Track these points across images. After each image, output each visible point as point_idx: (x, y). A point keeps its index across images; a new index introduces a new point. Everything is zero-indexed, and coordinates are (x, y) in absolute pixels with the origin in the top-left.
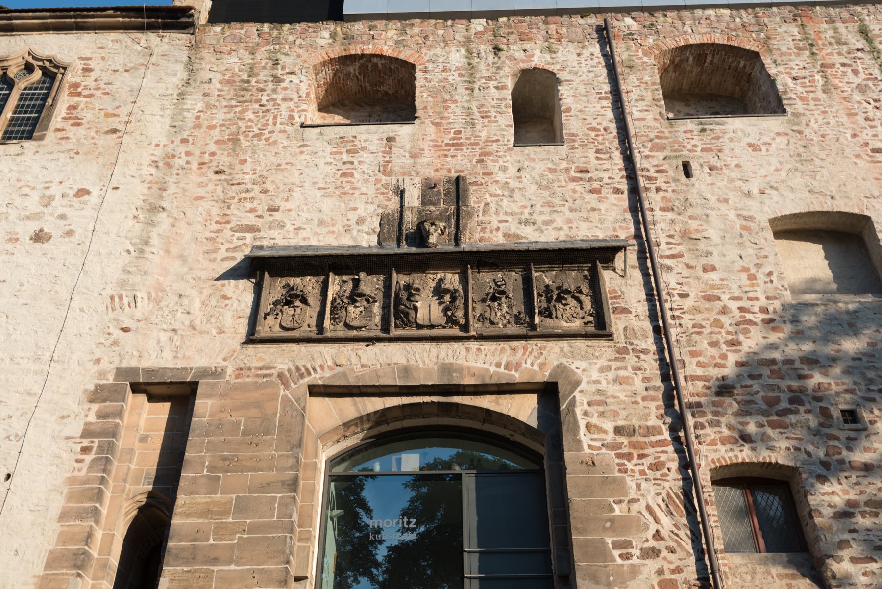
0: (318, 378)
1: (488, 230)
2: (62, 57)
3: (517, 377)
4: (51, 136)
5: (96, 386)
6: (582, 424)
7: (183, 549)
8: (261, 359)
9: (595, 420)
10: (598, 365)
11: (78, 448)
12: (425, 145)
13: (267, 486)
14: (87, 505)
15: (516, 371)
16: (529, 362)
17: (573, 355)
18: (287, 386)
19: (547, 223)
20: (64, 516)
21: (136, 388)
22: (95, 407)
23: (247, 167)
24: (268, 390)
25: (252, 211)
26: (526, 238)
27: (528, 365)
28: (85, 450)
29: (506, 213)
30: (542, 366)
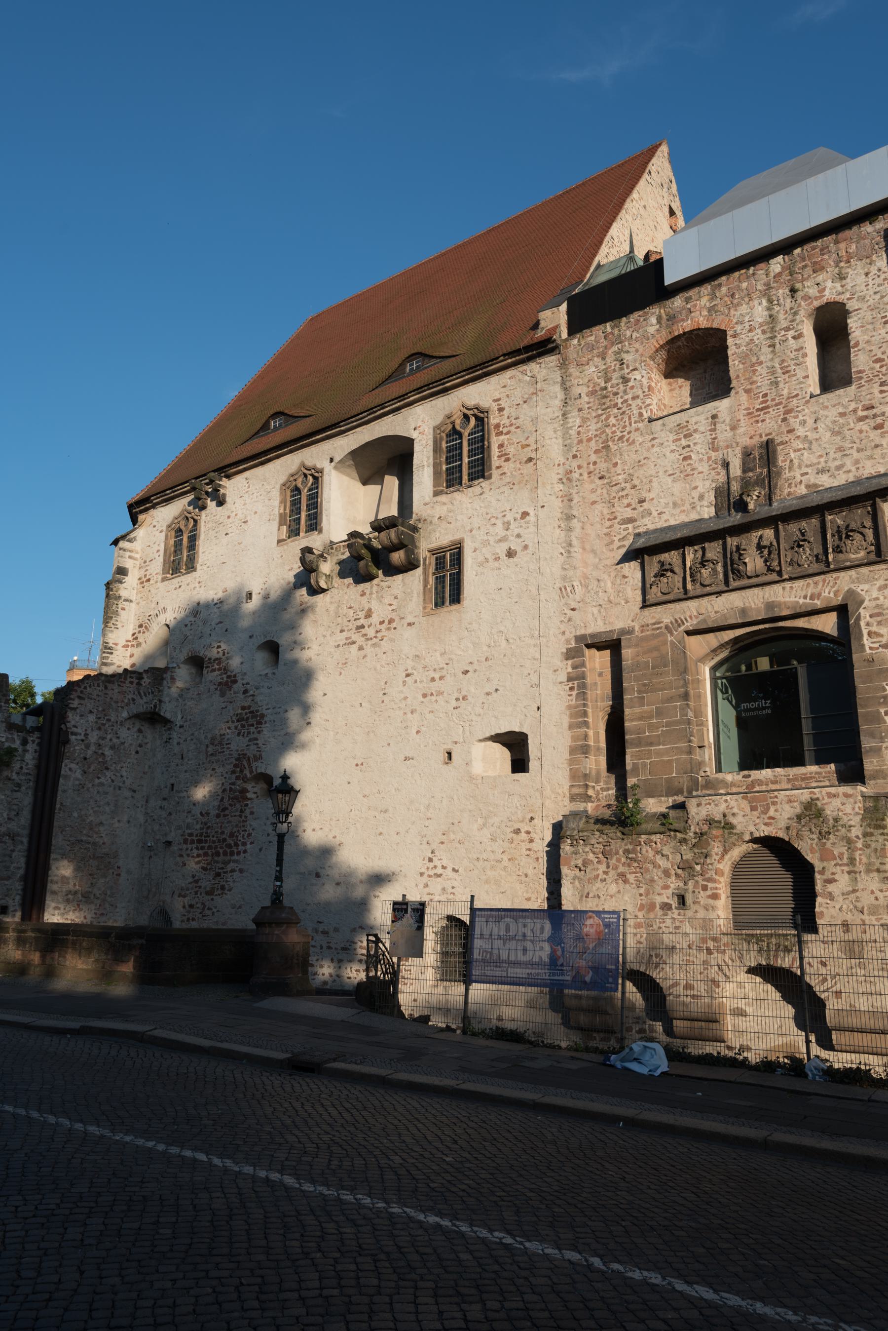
0: (689, 625)
1: (793, 485)
2: (485, 403)
3: (819, 604)
4: (495, 473)
5: (567, 649)
6: (865, 632)
7: (633, 739)
8: (653, 617)
9: (874, 628)
10: (878, 585)
11: (567, 688)
12: (741, 415)
13: (671, 699)
14: (580, 720)
15: (818, 599)
16: (827, 591)
17: (859, 581)
18: (672, 634)
19: (838, 468)
20: (571, 727)
21: (589, 646)
22: (570, 662)
23: (619, 469)
24: (661, 638)
25: (629, 505)
26: (822, 486)
27: (826, 594)
28: (571, 689)
29: (807, 466)
30: (836, 593)
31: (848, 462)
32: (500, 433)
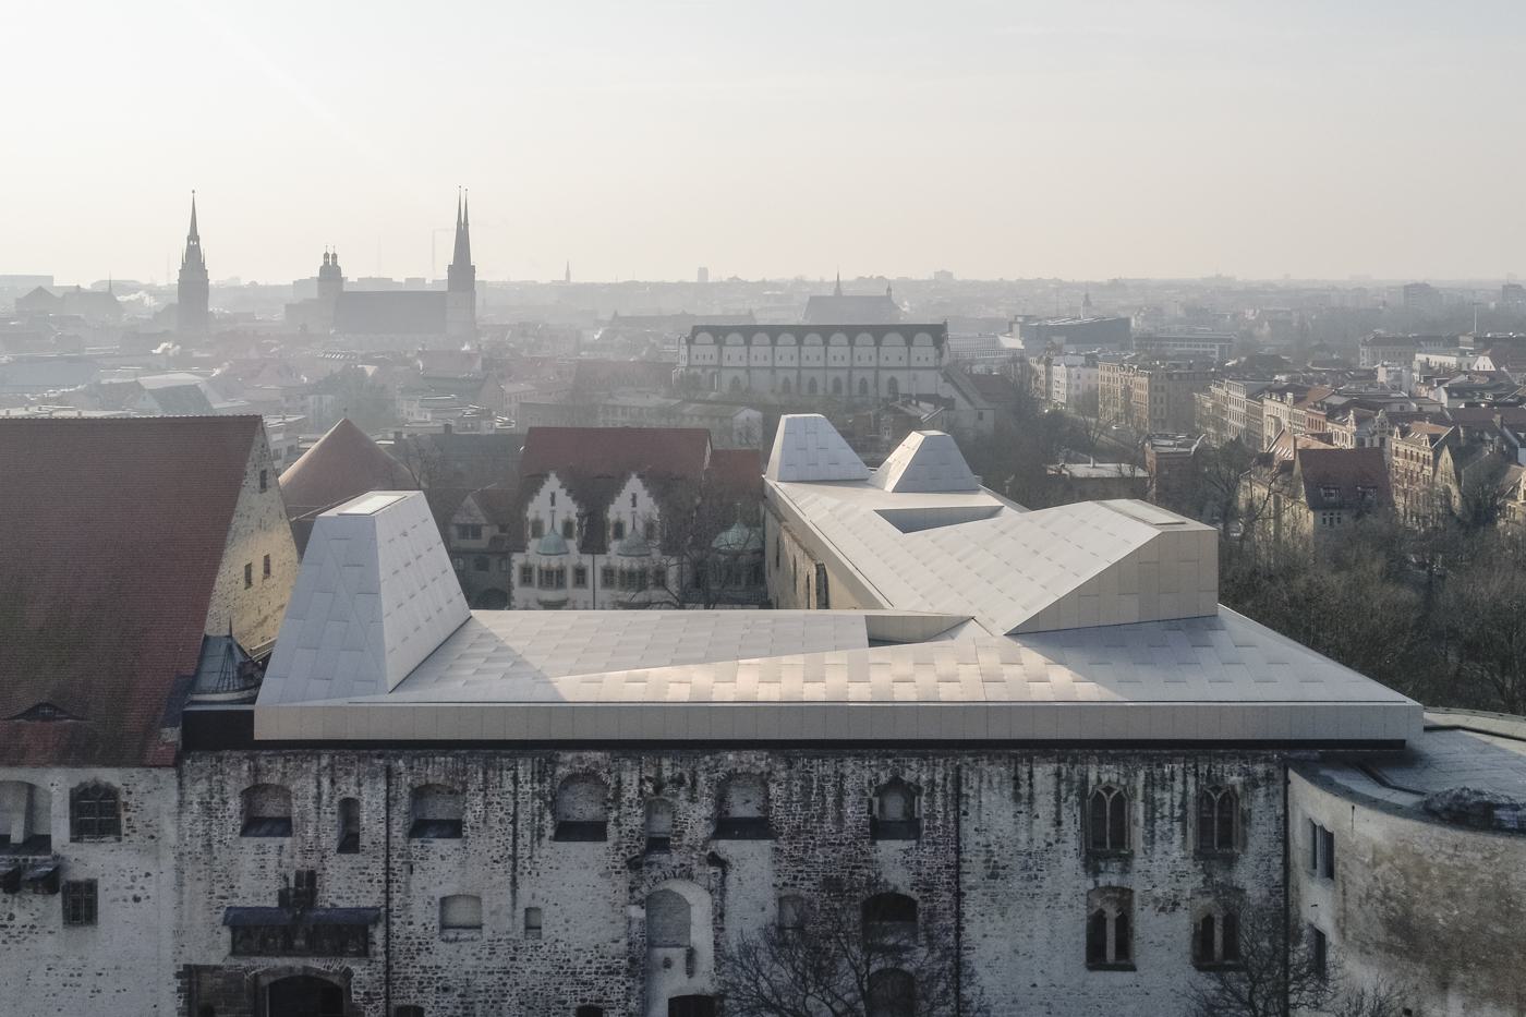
6: (353, 990)
12: (297, 850)
19: (348, 898)
22: (179, 981)
25: (223, 888)
28: (180, 997)
31: (354, 896)
32: (127, 810)
